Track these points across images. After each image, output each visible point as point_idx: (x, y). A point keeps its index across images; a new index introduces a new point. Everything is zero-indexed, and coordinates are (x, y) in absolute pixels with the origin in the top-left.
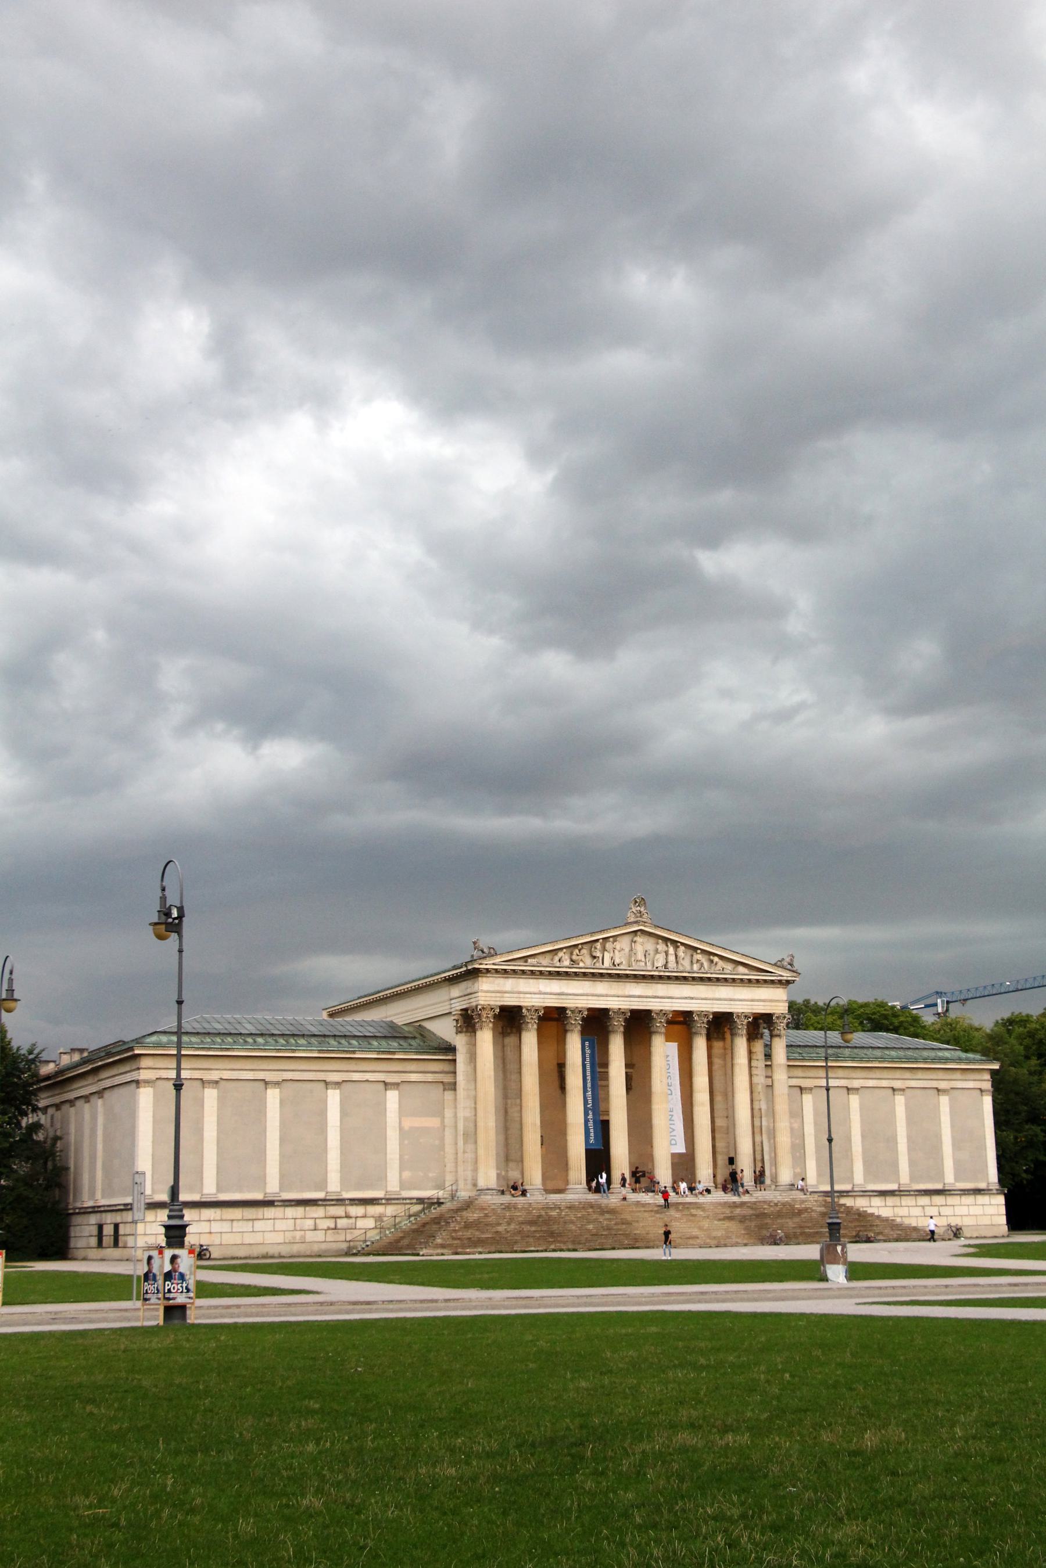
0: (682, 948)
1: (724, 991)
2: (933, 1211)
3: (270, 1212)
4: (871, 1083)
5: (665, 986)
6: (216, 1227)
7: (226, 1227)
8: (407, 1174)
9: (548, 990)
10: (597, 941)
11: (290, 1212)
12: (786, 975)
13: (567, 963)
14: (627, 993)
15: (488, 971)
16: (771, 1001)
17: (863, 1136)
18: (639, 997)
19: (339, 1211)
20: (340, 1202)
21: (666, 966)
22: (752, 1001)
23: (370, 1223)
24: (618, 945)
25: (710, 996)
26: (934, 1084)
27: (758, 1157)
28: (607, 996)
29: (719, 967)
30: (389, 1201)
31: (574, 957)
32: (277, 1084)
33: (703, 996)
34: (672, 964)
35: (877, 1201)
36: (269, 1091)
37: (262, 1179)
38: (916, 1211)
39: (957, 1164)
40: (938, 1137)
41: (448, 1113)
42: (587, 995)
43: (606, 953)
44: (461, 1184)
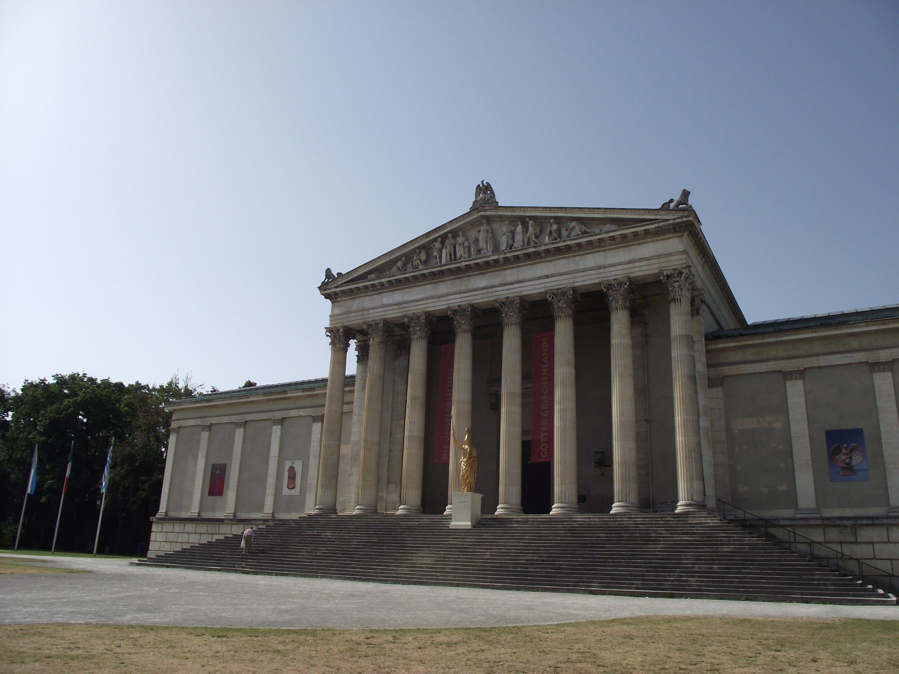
0: (531, 222)
1: (590, 260)
5: (515, 271)
9: (391, 301)
10: (435, 240)
12: (673, 218)
14: (470, 287)
16: (658, 257)
18: (483, 288)
22: (630, 262)
24: (460, 240)
25: (573, 267)
33: (562, 270)
34: (518, 244)
42: (427, 298)
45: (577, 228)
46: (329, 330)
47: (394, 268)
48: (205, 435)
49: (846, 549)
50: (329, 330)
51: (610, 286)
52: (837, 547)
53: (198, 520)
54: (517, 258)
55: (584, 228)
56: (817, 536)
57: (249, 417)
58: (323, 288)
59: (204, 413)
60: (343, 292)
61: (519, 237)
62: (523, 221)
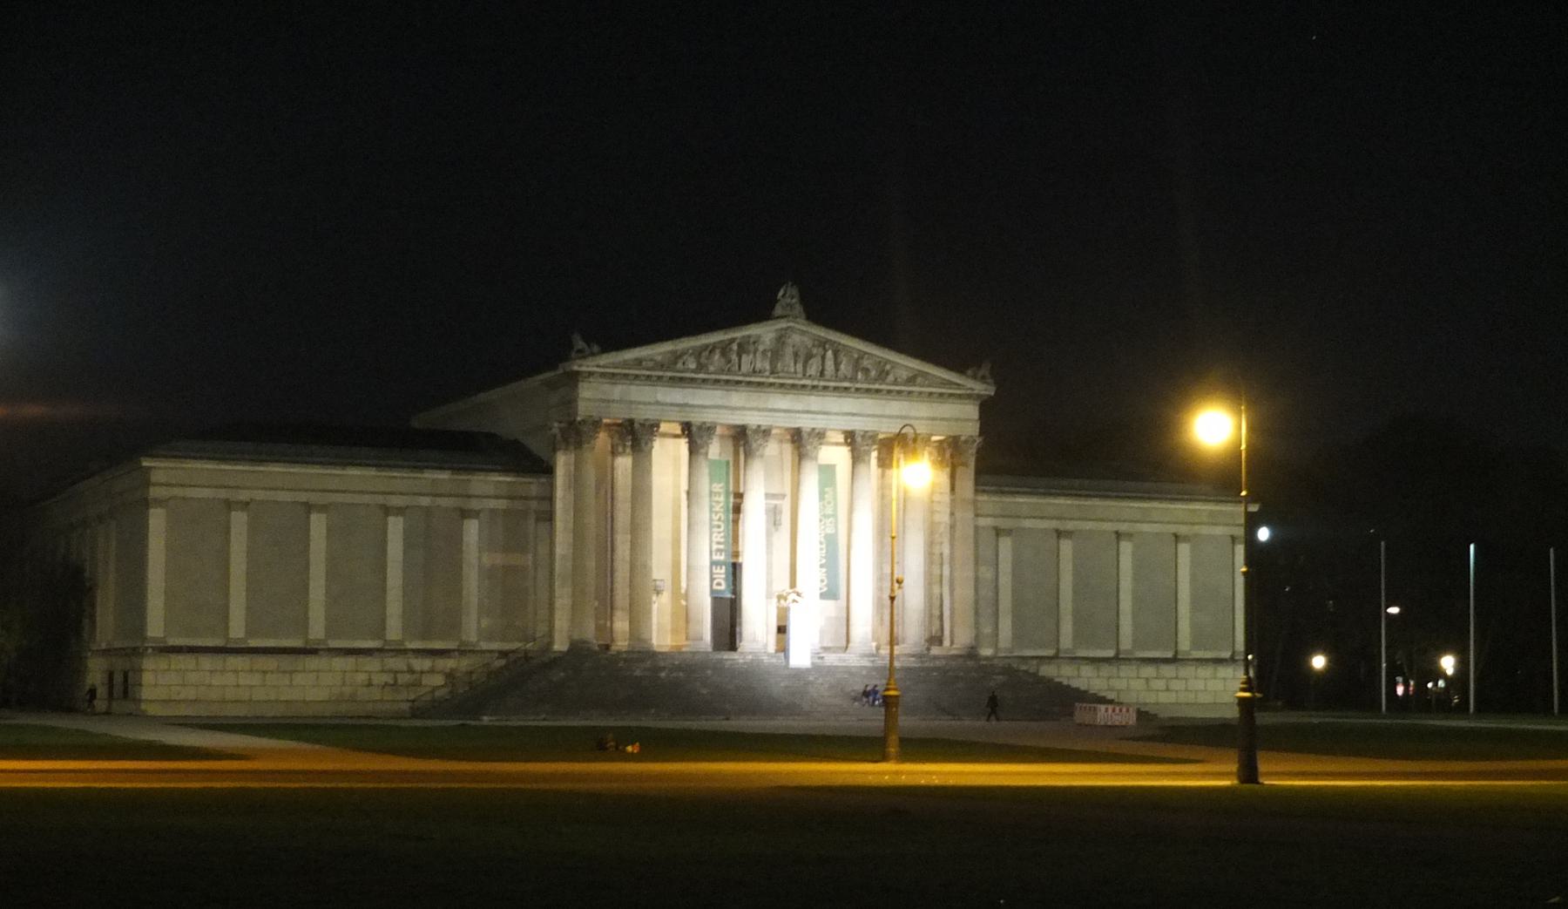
2: (1160, 684)
3: (312, 662)
4: (1089, 525)
6: (245, 680)
7: (256, 680)
8: (485, 623)
11: (339, 663)
13: (693, 366)
15: (591, 374)
17: (1075, 592)
19: (397, 663)
20: (403, 652)
21: (822, 373)
23: (439, 680)
26: (1172, 528)
27: (937, 613)
28: (743, 408)
29: (891, 378)
30: (462, 652)
31: (703, 360)
32: (323, 508)
35: (1087, 670)
36: (314, 517)
37: (303, 624)
38: (1138, 685)
39: (1194, 626)
41: (543, 550)
43: (744, 358)
44: (557, 636)
54: (825, 388)
61: (830, 364)
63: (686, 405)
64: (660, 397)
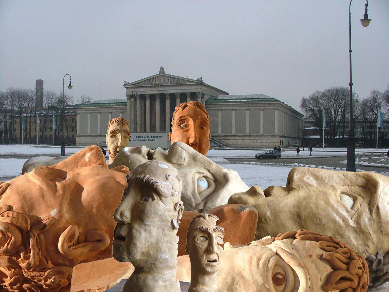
1: (184, 88)
2: (255, 141)
9: (141, 90)
12: (199, 82)
13: (145, 84)
34: (169, 82)
35: (237, 138)
40: (259, 121)
45: (182, 81)
46: (126, 95)
47: (142, 83)
48: (89, 115)
49: (225, 141)
50: (126, 95)
51: (187, 93)
52: (223, 140)
53: (90, 136)
55: (182, 81)
56: (220, 138)
57: (102, 111)
58: (124, 86)
59: (87, 110)
60: (130, 87)
61: (169, 81)
62: (170, 77)
63: (144, 91)
64: (140, 90)
